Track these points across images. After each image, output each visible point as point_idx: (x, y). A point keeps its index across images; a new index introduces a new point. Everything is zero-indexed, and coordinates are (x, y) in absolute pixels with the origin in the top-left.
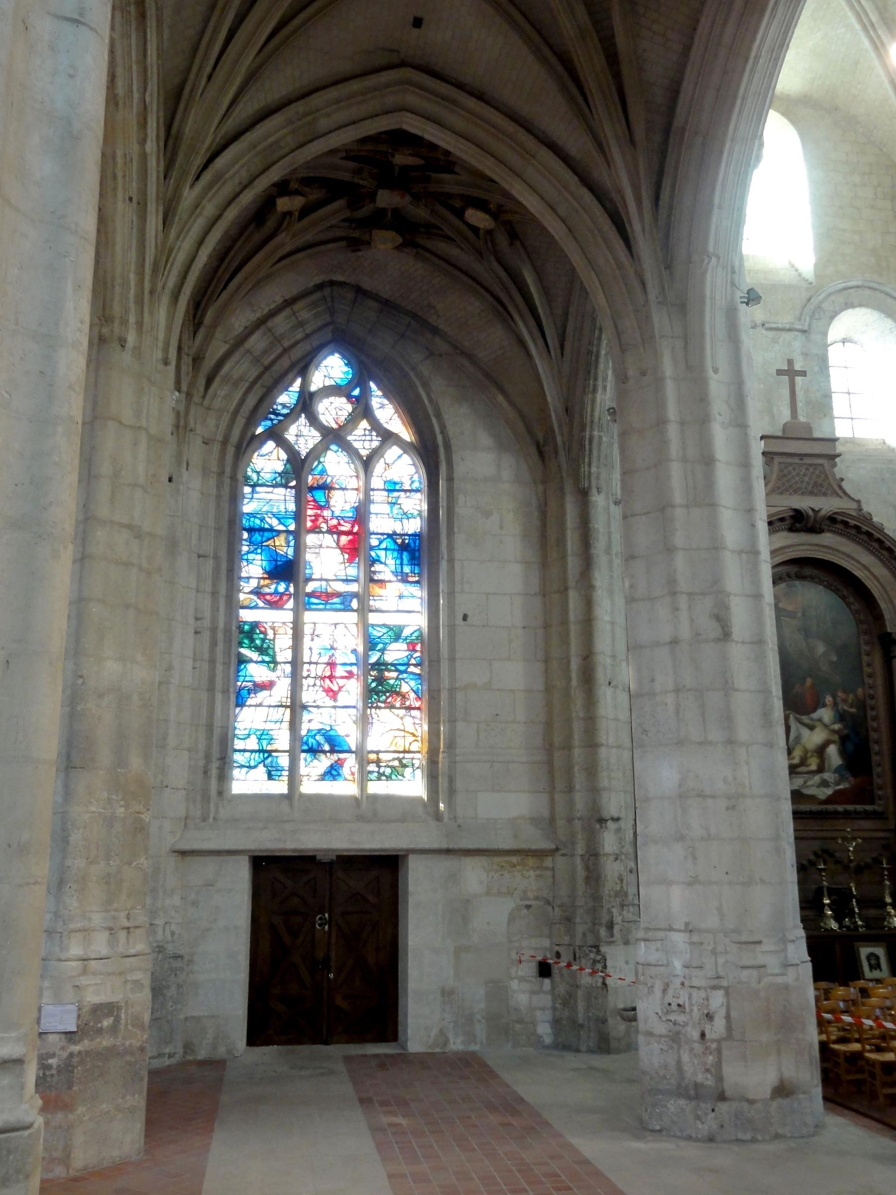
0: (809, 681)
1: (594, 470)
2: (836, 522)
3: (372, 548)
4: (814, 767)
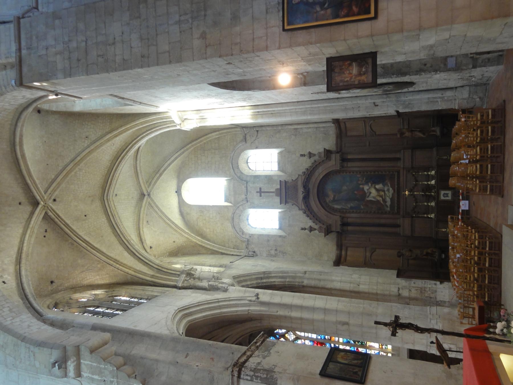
0: (356, 192)
1: (297, 284)
2: (305, 186)
3: (321, 338)
4: (383, 193)
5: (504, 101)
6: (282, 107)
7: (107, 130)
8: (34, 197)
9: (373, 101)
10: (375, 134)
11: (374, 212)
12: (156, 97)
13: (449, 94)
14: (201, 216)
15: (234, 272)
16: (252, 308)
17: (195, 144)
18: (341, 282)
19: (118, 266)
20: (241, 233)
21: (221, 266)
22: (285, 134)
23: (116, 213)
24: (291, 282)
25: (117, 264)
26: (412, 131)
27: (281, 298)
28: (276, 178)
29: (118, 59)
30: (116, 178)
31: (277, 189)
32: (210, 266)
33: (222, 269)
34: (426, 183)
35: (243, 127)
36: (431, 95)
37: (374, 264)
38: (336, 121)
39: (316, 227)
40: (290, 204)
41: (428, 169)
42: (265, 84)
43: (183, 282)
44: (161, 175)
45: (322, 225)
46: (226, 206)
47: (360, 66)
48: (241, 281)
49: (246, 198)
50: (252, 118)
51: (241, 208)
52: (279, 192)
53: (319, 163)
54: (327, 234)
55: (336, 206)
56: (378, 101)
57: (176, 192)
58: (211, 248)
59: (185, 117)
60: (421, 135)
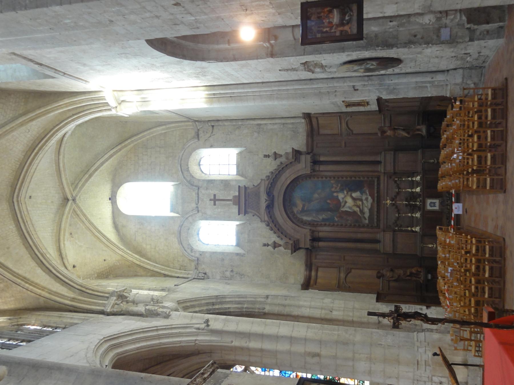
0: (329, 201)
1: (257, 310)
2: (269, 193)
4: (360, 203)
5: (506, 79)
6: (243, 88)
7: (21, 112)
9: (352, 84)
10: (353, 134)
11: (351, 225)
12: (84, 65)
13: (440, 77)
14: (140, 229)
15: (180, 296)
16: (200, 338)
17: (136, 140)
18: (310, 308)
19: (27, 285)
20: (189, 251)
21: (163, 290)
22: (245, 131)
23: (28, 220)
24: (250, 308)
25: (26, 283)
27: (237, 325)
28: (234, 183)
30: (31, 174)
31: (235, 197)
32: (149, 290)
33: (164, 294)
34: (410, 190)
36: (419, 79)
37: (349, 287)
38: (308, 116)
39: (281, 242)
40: (251, 215)
41: (413, 174)
43: (113, 307)
44: (91, 176)
45: (288, 241)
46: (172, 218)
48: (187, 306)
49: (197, 207)
50: (207, 102)
51: (190, 219)
52: (237, 201)
53: (286, 166)
54: (295, 252)
55: (305, 218)
56: (358, 84)
57: (110, 199)
58: (152, 268)
59: (122, 99)
60: (405, 134)
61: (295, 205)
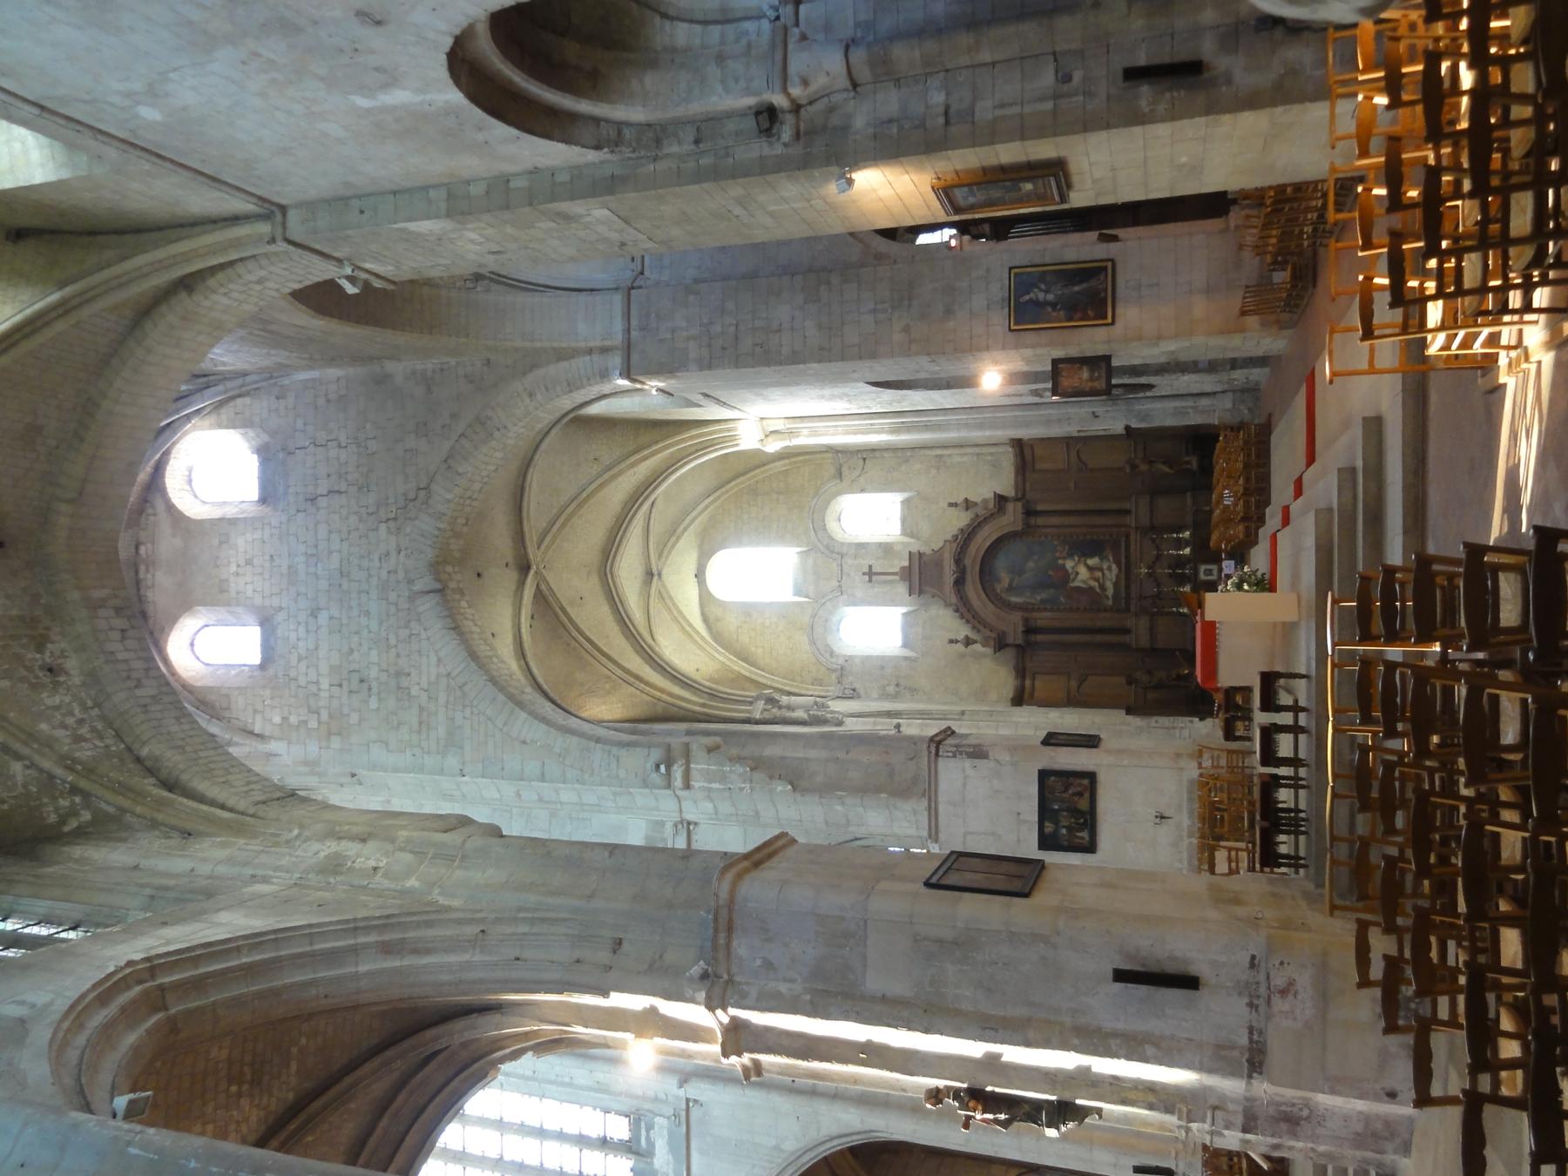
2: (958, 560)
8: (526, 555)
13: (1205, 402)
22: (918, 466)
26: (1151, 462)
29: (785, 350)
31: (903, 568)
35: (838, 452)
36: (1178, 403)
38: (1018, 444)
41: (1180, 529)
42: (965, 382)
45: (989, 634)
46: (799, 603)
47: (1092, 370)
52: (906, 574)
55: (1014, 599)
60: (1167, 469)
61: (999, 580)
